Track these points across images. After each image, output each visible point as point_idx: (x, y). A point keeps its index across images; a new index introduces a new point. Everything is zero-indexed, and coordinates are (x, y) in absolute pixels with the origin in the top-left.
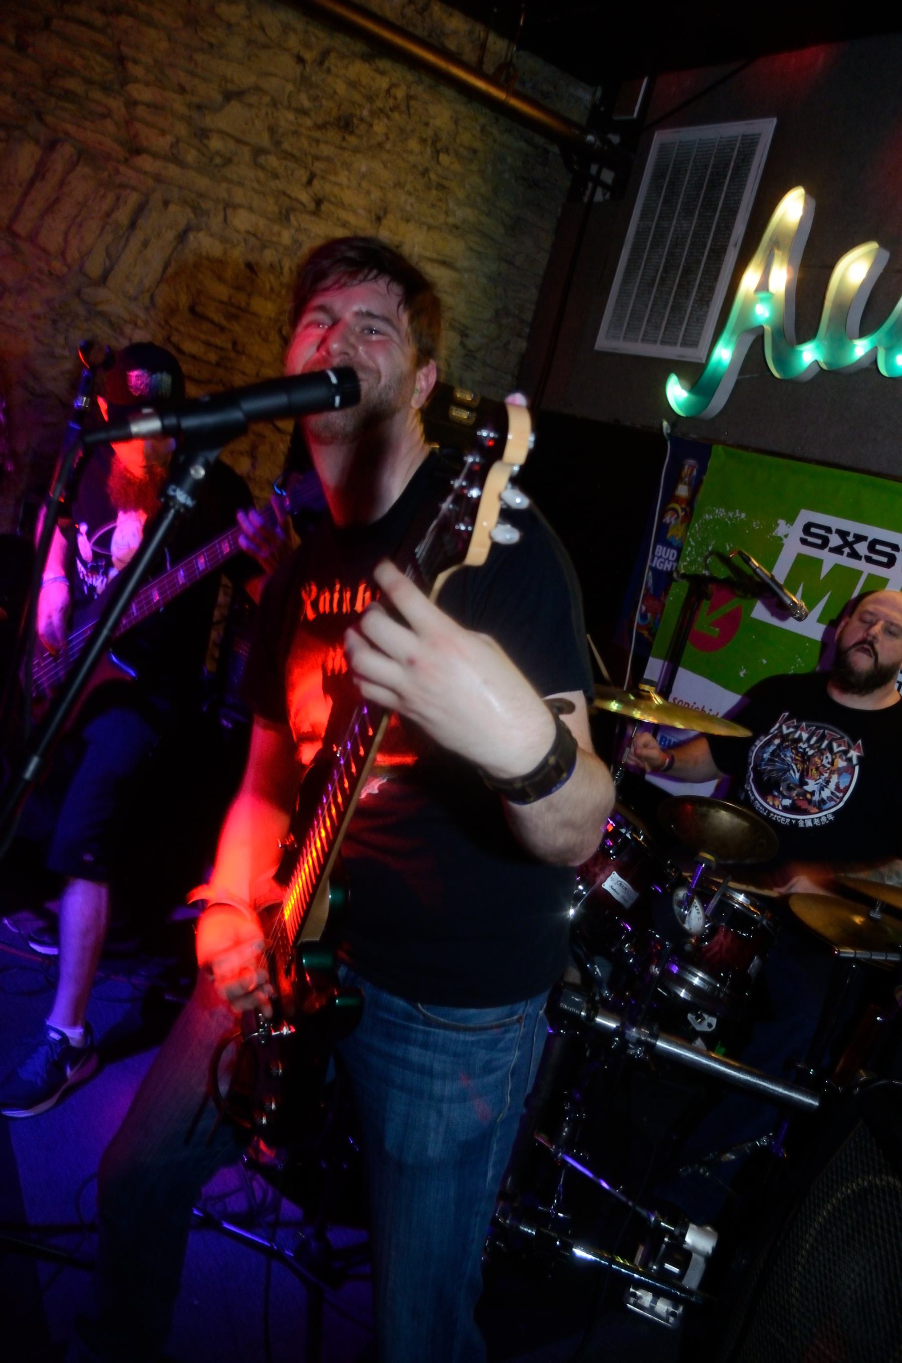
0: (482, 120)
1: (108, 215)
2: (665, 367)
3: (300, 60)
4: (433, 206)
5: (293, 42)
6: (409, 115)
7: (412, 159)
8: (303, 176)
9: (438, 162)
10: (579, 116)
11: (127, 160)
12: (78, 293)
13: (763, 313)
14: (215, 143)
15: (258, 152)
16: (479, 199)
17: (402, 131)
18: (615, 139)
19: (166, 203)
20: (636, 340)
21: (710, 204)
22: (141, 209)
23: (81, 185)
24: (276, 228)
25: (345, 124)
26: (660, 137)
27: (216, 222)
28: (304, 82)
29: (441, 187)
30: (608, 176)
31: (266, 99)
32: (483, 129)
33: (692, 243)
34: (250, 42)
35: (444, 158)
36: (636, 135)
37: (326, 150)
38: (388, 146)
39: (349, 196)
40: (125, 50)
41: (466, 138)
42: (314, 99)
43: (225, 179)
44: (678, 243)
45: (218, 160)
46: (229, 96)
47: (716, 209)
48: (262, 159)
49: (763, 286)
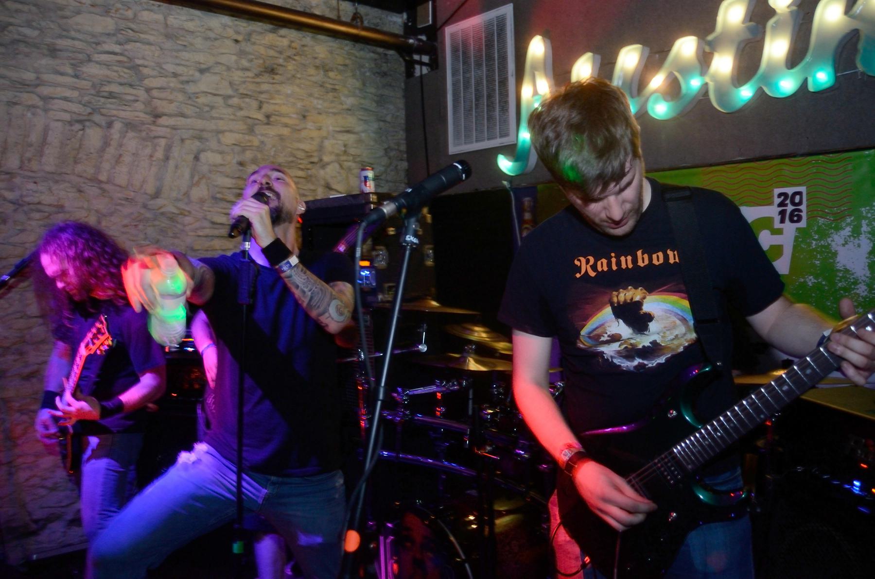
0: (346, 48)
1: (151, 156)
2: (493, 152)
3: (237, 41)
4: (332, 102)
5: (230, 32)
6: (306, 56)
7: (313, 79)
8: (255, 104)
9: (329, 78)
10: (398, 30)
11: (154, 122)
12: (145, 206)
14: (202, 100)
15: (227, 98)
16: (357, 91)
17: (304, 65)
18: (424, 38)
19: (183, 140)
20: (472, 142)
21: (490, 58)
22: (168, 148)
23: (132, 142)
24: (247, 137)
25: (272, 71)
27: (213, 144)
28: (242, 54)
29: (335, 90)
30: (426, 59)
31: (224, 68)
32: (349, 54)
33: (487, 81)
34: (207, 39)
35: (331, 74)
36: (434, 32)
37: (265, 87)
38: (299, 76)
39: (284, 109)
40: (139, 62)
41: (340, 60)
42: (251, 61)
43: (213, 118)
44: (478, 83)
45: (207, 109)
46: (202, 71)
47: (494, 60)
48: (230, 102)
49: (535, 93)
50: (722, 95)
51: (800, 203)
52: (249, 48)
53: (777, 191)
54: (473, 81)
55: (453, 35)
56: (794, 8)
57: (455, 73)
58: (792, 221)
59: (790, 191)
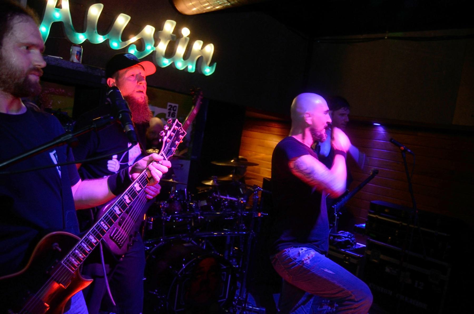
13: (57, 16)
50: (159, 58)
51: (175, 110)
56: (188, 38)
58: (172, 117)
59: (173, 105)
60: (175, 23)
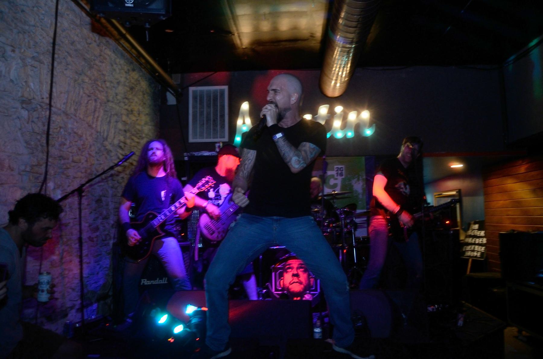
21: (215, 105)
26: (192, 89)
37: (130, 97)
44: (208, 114)
49: (244, 123)
52: (128, 77)
53: (336, 167)
54: (205, 113)
55: (194, 92)
56: (342, 113)
57: (194, 107)
59: (340, 166)
60: (328, 106)
